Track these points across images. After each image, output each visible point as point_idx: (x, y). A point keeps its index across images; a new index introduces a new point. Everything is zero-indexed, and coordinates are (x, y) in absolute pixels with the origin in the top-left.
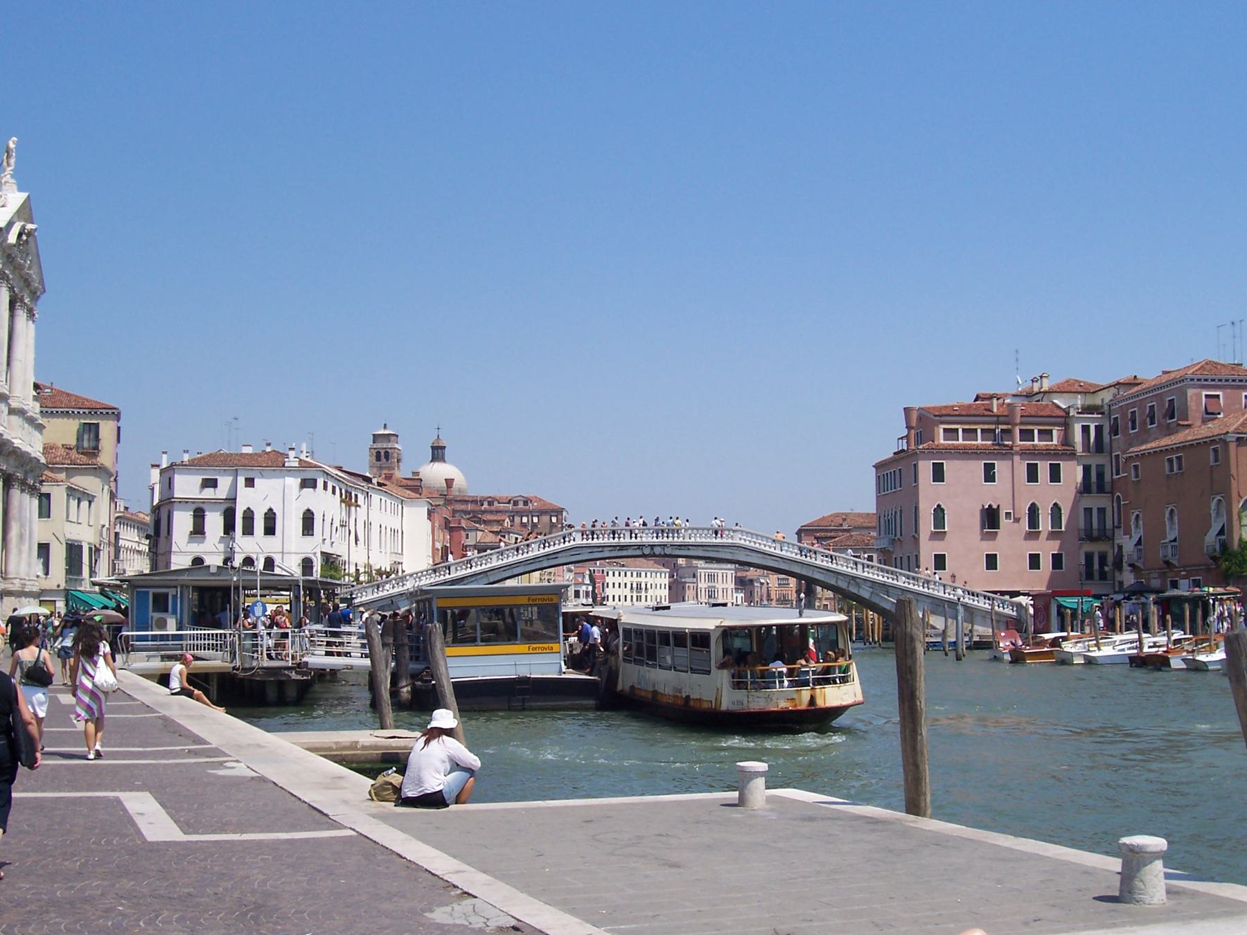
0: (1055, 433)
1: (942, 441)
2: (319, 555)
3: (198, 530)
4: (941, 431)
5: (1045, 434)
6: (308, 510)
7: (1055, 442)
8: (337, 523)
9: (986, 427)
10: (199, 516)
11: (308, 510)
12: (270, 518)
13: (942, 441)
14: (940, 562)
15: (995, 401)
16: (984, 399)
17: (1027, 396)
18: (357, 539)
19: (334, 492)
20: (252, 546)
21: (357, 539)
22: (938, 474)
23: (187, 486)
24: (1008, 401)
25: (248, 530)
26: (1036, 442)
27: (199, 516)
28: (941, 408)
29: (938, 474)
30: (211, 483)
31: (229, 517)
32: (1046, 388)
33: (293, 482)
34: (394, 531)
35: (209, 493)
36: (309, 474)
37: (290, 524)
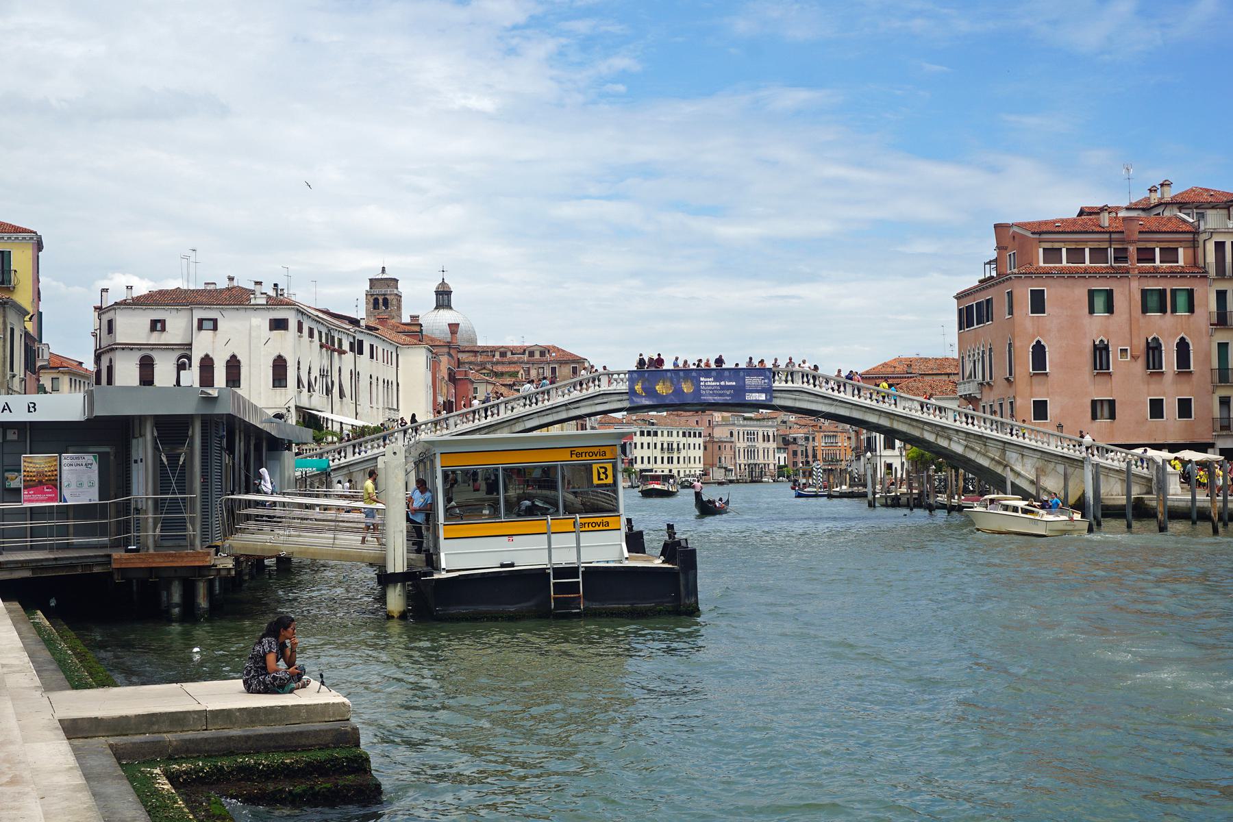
0: (1181, 251)
1: (1041, 264)
2: (293, 410)
4: (1041, 251)
5: (1170, 254)
6: (280, 357)
7: (1181, 263)
9: (1095, 245)
11: (280, 357)
12: (233, 366)
13: (1041, 264)
14: (1040, 410)
15: (1106, 214)
16: (1090, 214)
17: (1143, 210)
18: (342, 395)
19: (311, 335)
21: (342, 395)
22: (1038, 302)
23: (132, 328)
24: (1122, 214)
26: (1158, 263)
28: (1040, 223)
29: (1038, 302)
30: (157, 325)
32: (1167, 198)
33: (260, 322)
34: (387, 383)
35: (155, 338)
36: (279, 314)
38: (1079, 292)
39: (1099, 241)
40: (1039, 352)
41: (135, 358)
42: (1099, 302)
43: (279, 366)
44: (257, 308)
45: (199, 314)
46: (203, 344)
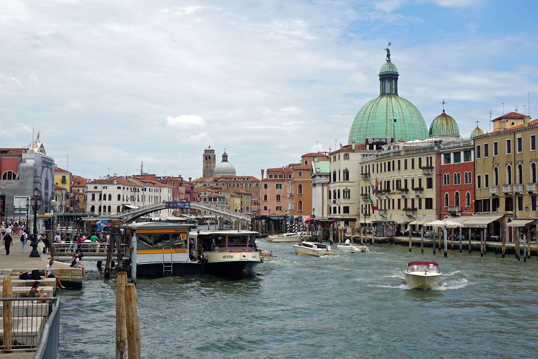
3: (93, 199)
8: (129, 197)
10: (93, 196)
12: (110, 196)
14: (266, 208)
20: (106, 203)
21: (138, 201)
22: (266, 187)
25: (105, 199)
27: (93, 196)
29: (266, 187)
30: (96, 188)
31: (101, 195)
33: (116, 187)
36: (119, 186)
37: (114, 198)
38: (274, 184)
39: (281, 174)
40: (266, 196)
41: (91, 194)
42: (279, 186)
43: (119, 196)
44: (115, 184)
45: (104, 185)
46: (104, 192)
